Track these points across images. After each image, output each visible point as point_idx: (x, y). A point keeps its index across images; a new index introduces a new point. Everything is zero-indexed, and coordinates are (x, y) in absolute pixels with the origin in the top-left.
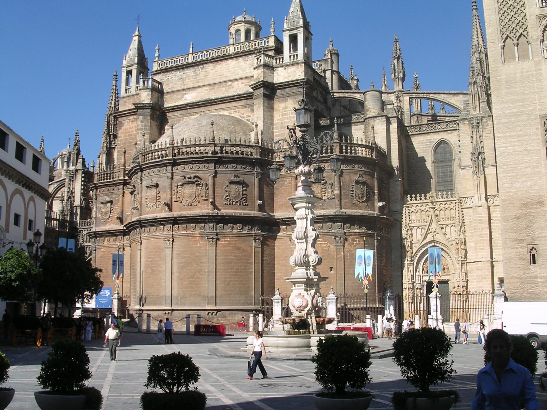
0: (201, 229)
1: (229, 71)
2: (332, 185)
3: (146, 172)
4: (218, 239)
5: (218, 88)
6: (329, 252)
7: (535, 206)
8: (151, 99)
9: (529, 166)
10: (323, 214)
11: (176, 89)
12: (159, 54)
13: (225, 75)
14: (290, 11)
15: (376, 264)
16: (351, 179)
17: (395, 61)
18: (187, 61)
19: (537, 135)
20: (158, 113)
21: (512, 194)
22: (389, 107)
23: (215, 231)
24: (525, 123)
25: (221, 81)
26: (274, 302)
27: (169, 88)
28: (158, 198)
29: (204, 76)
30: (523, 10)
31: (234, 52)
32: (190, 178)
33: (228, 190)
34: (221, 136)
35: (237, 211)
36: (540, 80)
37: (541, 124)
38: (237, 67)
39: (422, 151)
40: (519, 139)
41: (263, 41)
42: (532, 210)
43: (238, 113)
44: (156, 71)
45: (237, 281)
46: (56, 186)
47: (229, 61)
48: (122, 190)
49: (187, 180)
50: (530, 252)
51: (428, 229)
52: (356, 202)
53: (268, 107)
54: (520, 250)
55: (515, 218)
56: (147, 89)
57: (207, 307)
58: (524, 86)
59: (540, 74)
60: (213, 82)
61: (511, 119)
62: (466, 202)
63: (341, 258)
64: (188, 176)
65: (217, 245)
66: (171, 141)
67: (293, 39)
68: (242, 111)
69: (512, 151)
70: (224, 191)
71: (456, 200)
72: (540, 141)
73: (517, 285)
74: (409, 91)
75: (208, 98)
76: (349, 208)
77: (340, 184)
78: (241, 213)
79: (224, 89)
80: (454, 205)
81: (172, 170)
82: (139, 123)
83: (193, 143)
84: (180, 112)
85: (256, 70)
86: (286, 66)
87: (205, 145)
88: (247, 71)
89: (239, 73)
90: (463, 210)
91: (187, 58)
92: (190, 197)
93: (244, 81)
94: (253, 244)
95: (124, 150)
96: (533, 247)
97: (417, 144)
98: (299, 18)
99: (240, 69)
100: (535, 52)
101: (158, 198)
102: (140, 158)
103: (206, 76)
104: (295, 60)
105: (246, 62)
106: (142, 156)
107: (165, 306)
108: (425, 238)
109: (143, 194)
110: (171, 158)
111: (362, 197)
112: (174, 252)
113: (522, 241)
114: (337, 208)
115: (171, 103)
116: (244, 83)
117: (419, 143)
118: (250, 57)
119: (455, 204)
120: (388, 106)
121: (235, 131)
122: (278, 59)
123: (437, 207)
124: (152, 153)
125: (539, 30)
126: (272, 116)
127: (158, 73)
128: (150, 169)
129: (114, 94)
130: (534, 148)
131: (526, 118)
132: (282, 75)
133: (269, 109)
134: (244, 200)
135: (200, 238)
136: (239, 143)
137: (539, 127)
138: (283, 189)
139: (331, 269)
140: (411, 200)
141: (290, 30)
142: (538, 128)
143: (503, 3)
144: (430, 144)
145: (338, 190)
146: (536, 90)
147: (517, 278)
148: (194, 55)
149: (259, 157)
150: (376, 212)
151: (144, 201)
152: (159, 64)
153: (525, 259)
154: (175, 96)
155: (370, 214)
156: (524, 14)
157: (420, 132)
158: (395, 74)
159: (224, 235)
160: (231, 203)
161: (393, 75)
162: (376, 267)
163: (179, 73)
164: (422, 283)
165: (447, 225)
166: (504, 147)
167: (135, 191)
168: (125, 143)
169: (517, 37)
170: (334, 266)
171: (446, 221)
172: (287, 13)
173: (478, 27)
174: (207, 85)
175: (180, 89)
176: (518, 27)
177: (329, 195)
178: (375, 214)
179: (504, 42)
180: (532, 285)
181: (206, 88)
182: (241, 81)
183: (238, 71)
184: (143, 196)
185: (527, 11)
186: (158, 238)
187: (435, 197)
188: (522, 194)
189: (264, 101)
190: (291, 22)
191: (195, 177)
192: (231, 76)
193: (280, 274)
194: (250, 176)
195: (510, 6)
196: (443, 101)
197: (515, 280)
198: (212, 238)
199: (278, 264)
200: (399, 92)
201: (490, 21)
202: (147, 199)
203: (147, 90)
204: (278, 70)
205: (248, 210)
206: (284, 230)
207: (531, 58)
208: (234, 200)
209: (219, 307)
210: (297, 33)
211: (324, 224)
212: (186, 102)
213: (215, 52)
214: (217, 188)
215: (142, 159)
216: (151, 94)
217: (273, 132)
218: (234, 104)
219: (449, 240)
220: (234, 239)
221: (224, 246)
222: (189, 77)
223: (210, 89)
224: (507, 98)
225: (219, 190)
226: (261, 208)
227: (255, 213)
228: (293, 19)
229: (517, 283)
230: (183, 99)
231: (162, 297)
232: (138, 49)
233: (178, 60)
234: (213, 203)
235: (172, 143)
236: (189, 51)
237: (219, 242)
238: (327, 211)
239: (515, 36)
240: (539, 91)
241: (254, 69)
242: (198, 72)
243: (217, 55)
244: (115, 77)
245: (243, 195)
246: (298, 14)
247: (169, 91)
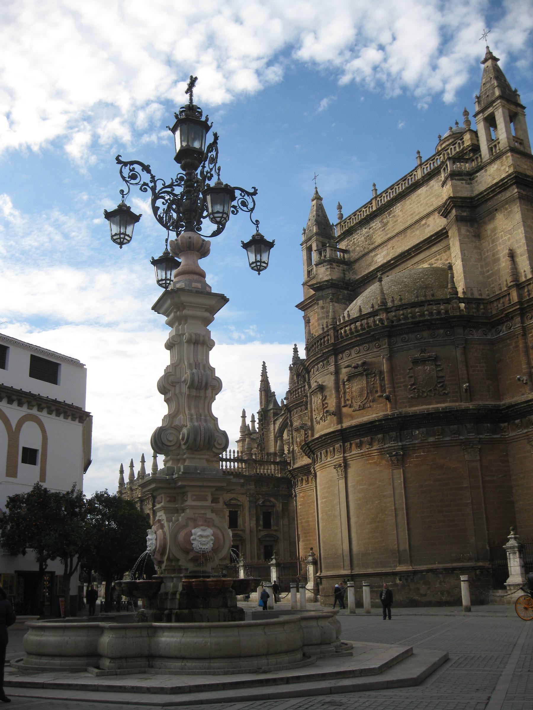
1: (421, 205)
13: (417, 213)
20: (346, 292)
33: (413, 375)
41: (457, 145)
46: (281, 420)
56: (324, 261)
70: (407, 379)
79: (418, 232)
91: (370, 206)
103: (395, 222)
112: (350, 485)
152: (343, 226)
183: (432, 200)
189: (459, 230)
204: (477, 176)
205: (450, 402)
208: (424, 390)
213: (402, 184)
218: (434, 249)
242: (385, 221)
246: (492, 83)
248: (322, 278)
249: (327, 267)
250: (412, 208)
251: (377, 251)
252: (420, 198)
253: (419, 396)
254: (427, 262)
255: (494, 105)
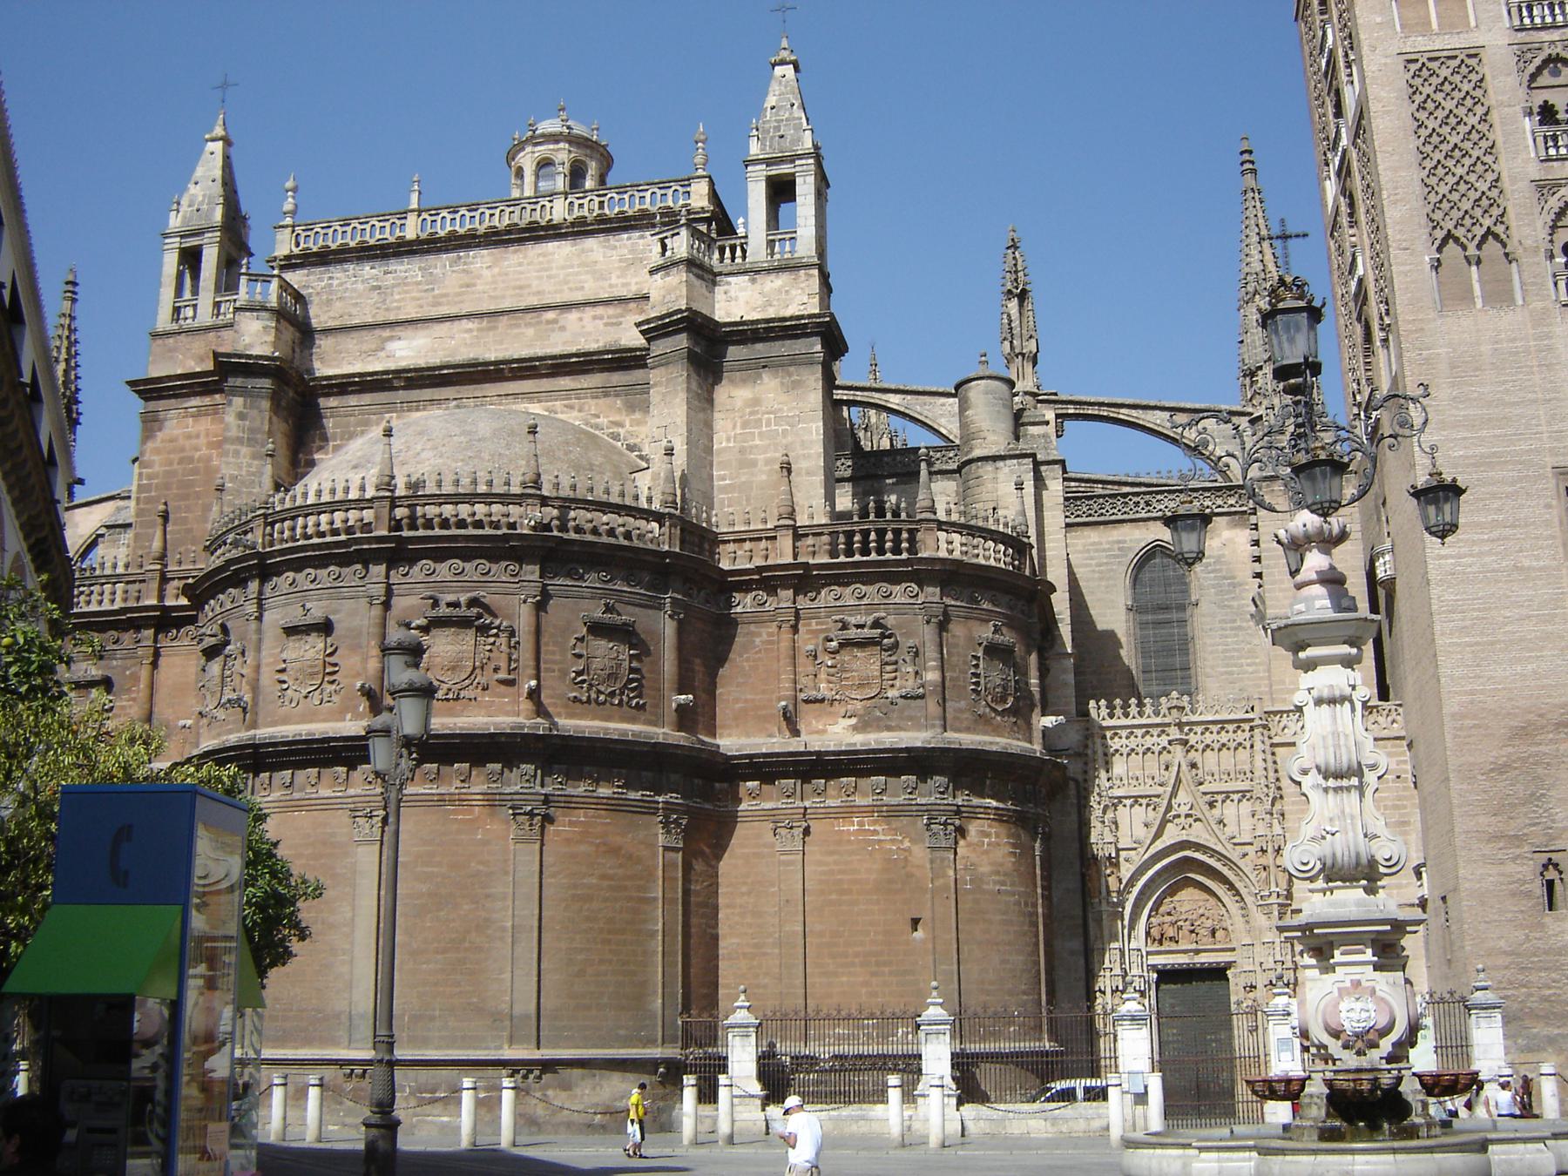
0: (489, 781)
1: (549, 277)
2: (917, 654)
3: (283, 581)
4: (548, 819)
5: (511, 326)
6: (908, 869)
7: (1551, 736)
8: (275, 345)
9: (1529, 617)
10: (888, 746)
11: (356, 321)
12: (296, 205)
13: (534, 289)
14: (768, 105)
15: (1040, 910)
16: (970, 638)
17: (1013, 305)
18: (398, 233)
19: (1547, 524)
20: (291, 394)
21: (1482, 697)
22: (1033, 430)
23: (538, 788)
24: (1510, 489)
25: (522, 305)
26: (730, 1035)
27: (332, 314)
28: (328, 670)
29: (461, 286)
30: (1490, 162)
31: (570, 219)
32: (456, 605)
34: (559, 478)
35: (612, 725)
36: (1549, 366)
37: (1558, 491)
38: (579, 266)
39: (1097, 575)
40: (1495, 534)
42: (1542, 748)
43: (580, 411)
44: (287, 258)
45: (610, 962)
47: (551, 246)
48: (150, 643)
49: (443, 611)
50: (1542, 874)
51: (1169, 807)
52: (988, 710)
53: (698, 394)
54: (1510, 868)
55: (1492, 770)
56: (264, 309)
57: (508, 1053)
58: (1505, 382)
59: (1550, 348)
60: (492, 307)
61: (1470, 474)
62: (1282, 725)
63: (946, 888)
64: (451, 598)
65: (546, 838)
66: (387, 479)
67: (781, 191)
68: (592, 405)
69: (1475, 569)
70: (570, 656)
71: (1252, 720)
72: (1559, 542)
73: (1508, 973)
74: (1056, 394)
75: (472, 356)
76: (968, 730)
77: (942, 654)
78: (625, 732)
79: (530, 332)
80: (1247, 734)
81: (388, 577)
82: (230, 418)
83: (448, 489)
84: (367, 398)
85: (658, 276)
86: (758, 272)
87: (506, 499)
88: (614, 281)
89: (586, 285)
90: (1277, 750)
92: (453, 669)
93: (600, 310)
94: (661, 838)
95: (162, 507)
96: (1550, 859)
97: (1080, 552)
98: (798, 128)
99: (587, 273)
100: (1534, 284)
101: (328, 670)
102: (259, 532)
103: (468, 286)
104: (777, 257)
105: (609, 253)
106: (266, 524)
107: (349, 1047)
108: (1158, 835)
109: (264, 653)
110: (385, 533)
111: (1003, 700)
113: (1517, 839)
114: (933, 726)
115: (338, 366)
116: (601, 318)
117: (1088, 551)
118: (625, 236)
119: (1252, 729)
120: (1030, 428)
121: (591, 465)
122: (728, 250)
123: (1192, 739)
124: (294, 518)
125: (1539, 224)
126: (709, 425)
127: (290, 263)
128: (298, 570)
129: (65, 343)
130: (1542, 563)
131: (1516, 474)
132: (742, 301)
133: (703, 401)
134: (633, 690)
135: (487, 810)
136: (618, 500)
137: (1554, 503)
138: (748, 660)
139: (915, 923)
140: (1141, 714)
141: (769, 162)
142: (1548, 506)
143: (1432, 140)
144: (1122, 556)
145: (934, 668)
146: (1540, 396)
147: (1505, 953)
148: (424, 215)
149: (677, 550)
150: (1037, 748)
151: (267, 678)
153: (1528, 894)
154: (350, 342)
155: (1026, 749)
156: (1495, 176)
157: (1090, 519)
158: (1011, 342)
159: (570, 804)
160: (593, 696)
161: (1007, 344)
162: (1041, 920)
163: (368, 270)
164: (1145, 974)
165: (1227, 795)
166: (1452, 557)
167: (228, 643)
168: (167, 486)
169: (1478, 238)
170: (926, 915)
171: (1239, 783)
172: (760, 111)
173: (1261, 221)
174: (469, 316)
175: (369, 320)
176: (1478, 212)
177: (910, 685)
178: (1035, 751)
179: (1439, 250)
180: (1553, 975)
181: (466, 324)
182: (590, 312)
184: (265, 661)
185: (1504, 166)
186: (326, 806)
187: (1188, 709)
188: (1510, 699)
190: (772, 138)
191: (473, 602)
192: (556, 292)
193: (734, 940)
194: (650, 612)
195: (1452, 150)
196: (1160, 429)
197: (1502, 961)
198: (531, 814)
199: (728, 906)
200: (1028, 397)
201: (1396, 188)
202: (282, 671)
203: (263, 314)
204: (729, 283)
206: (752, 795)
207: (1520, 302)
208: (602, 688)
209: (546, 1053)
210: (793, 175)
211: (891, 780)
212: (392, 366)
214: (547, 644)
215: (264, 536)
216: (277, 329)
217: (711, 477)
218: (565, 382)
219: (1235, 841)
220: (599, 817)
221: (568, 841)
222: (405, 284)
223: (479, 330)
224: (1456, 413)
225: (553, 653)
226: (685, 718)
227: (665, 733)
228: (777, 128)
229: (1506, 968)
230: (382, 354)
231: (338, 1016)
232: (225, 184)
233: (368, 227)
234: (534, 695)
235: (388, 483)
236: (408, 202)
237: (551, 828)
238: (903, 734)
239: (1470, 236)
240: (1548, 397)
241: (651, 272)
243: (507, 222)
244: (70, 288)
245: (632, 670)
247: (332, 324)
248: (251, 346)
249: (269, 323)
250: (522, 273)
251: (398, 331)
252: (549, 262)
253: (589, 701)
254: (540, 401)
255: (798, 162)
